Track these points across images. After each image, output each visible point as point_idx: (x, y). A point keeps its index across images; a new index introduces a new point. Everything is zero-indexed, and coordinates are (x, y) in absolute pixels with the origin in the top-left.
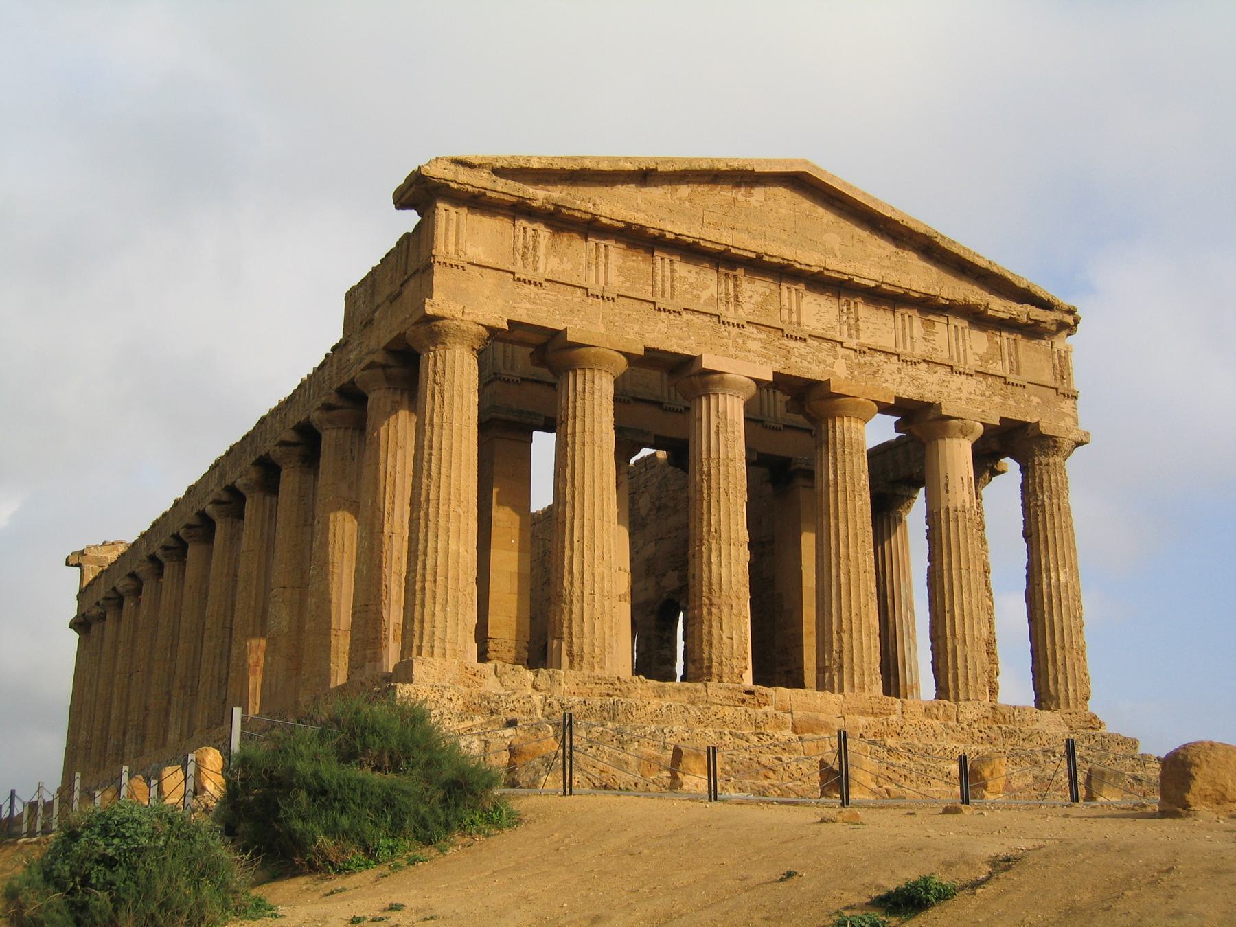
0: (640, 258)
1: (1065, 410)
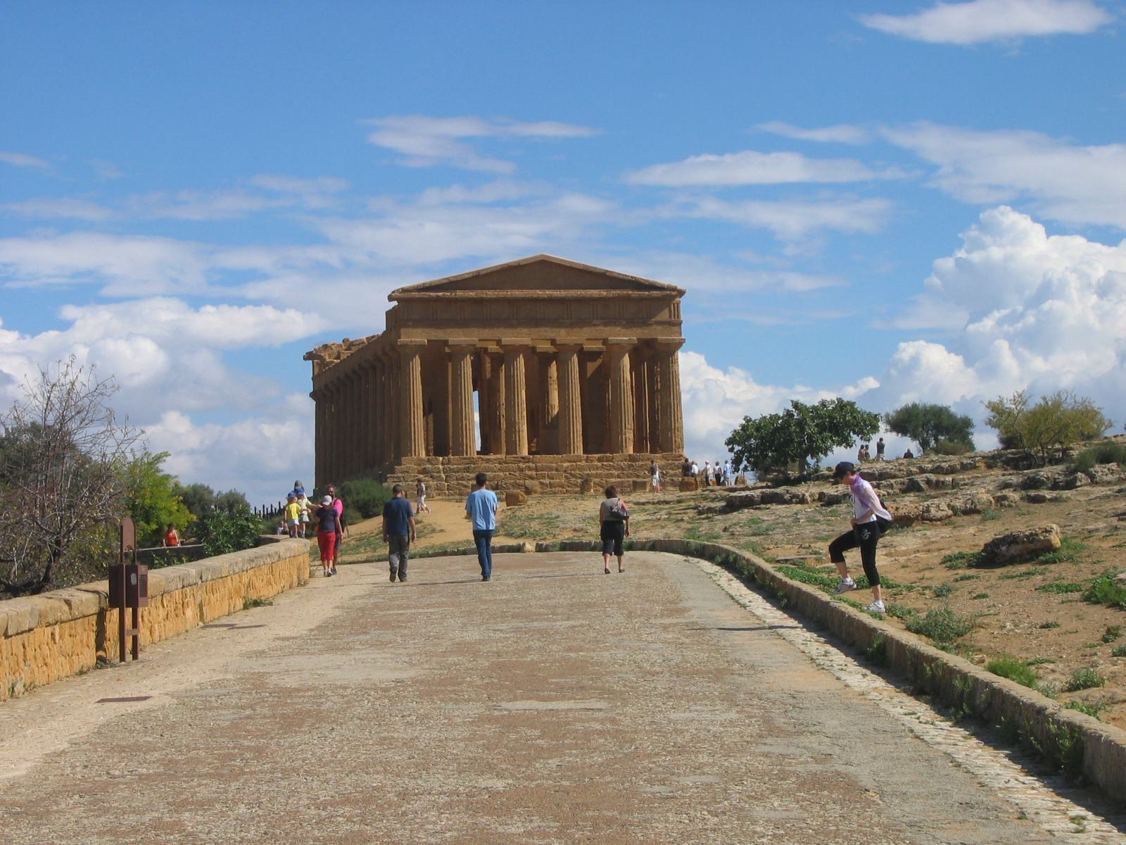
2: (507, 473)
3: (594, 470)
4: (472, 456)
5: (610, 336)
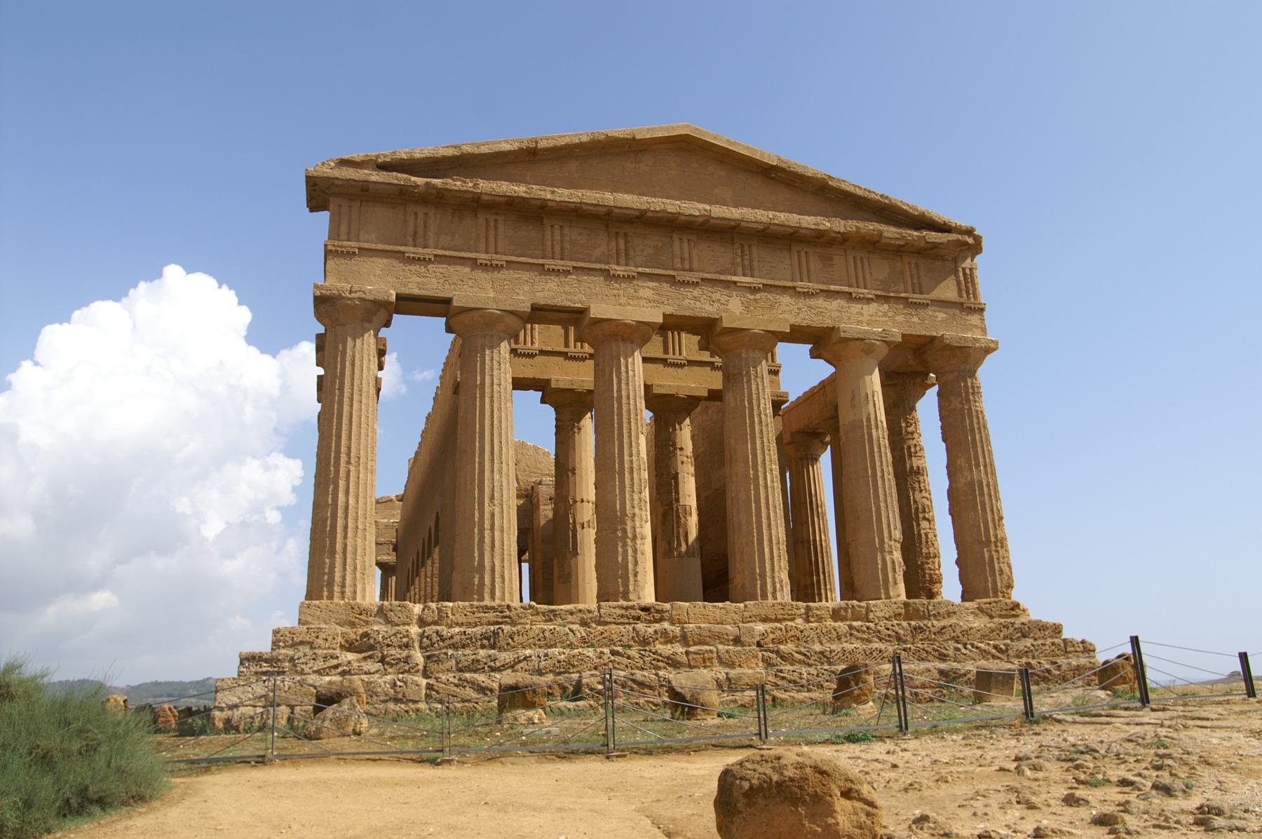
0: (531, 227)
1: (973, 322)
2: (606, 650)
3: (830, 640)
4: (507, 602)
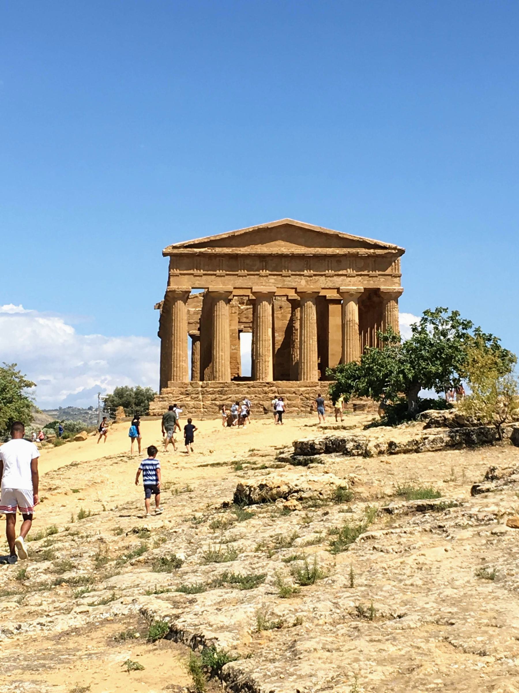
2: (253, 396)
5: (342, 285)
